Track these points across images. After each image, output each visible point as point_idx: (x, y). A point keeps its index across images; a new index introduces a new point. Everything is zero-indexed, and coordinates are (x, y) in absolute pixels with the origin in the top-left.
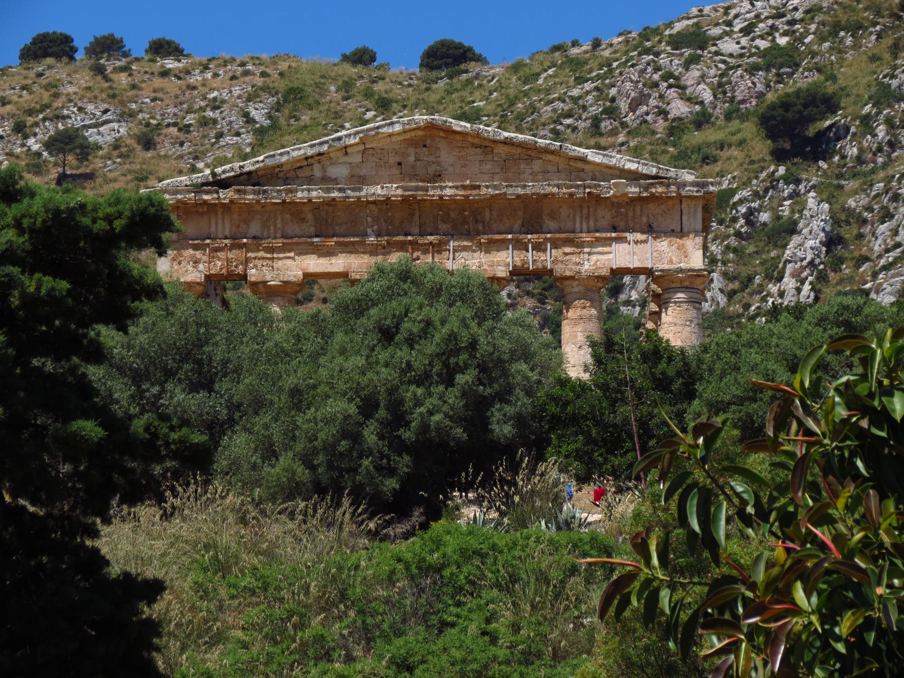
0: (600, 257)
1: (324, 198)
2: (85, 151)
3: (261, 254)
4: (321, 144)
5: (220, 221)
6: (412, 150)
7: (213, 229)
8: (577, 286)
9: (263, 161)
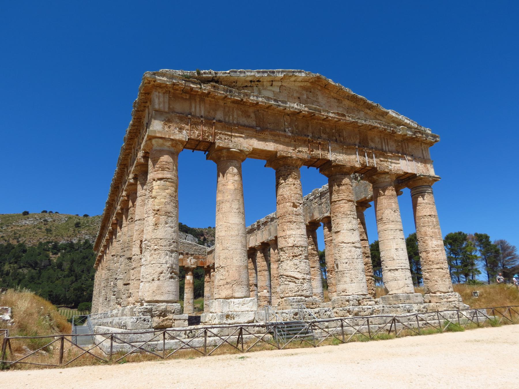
0: (395, 165)
1: (265, 103)
2: (47, 221)
4: (263, 72)
5: (198, 106)
6: (304, 92)
7: (193, 110)
8: (388, 178)
9: (229, 73)
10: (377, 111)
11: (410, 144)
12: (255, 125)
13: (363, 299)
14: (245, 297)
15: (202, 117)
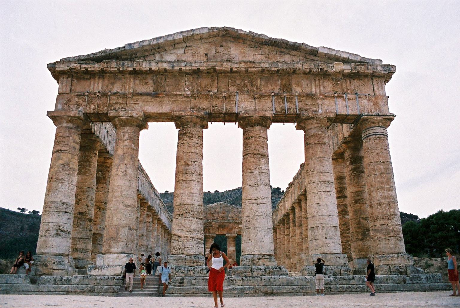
3: (119, 101)
5: (97, 83)
6: (214, 48)
7: (92, 87)
10: (305, 51)
11: (352, 81)
12: (152, 91)
13: (260, 259)
14: (121, 253)
15: (99, 92)
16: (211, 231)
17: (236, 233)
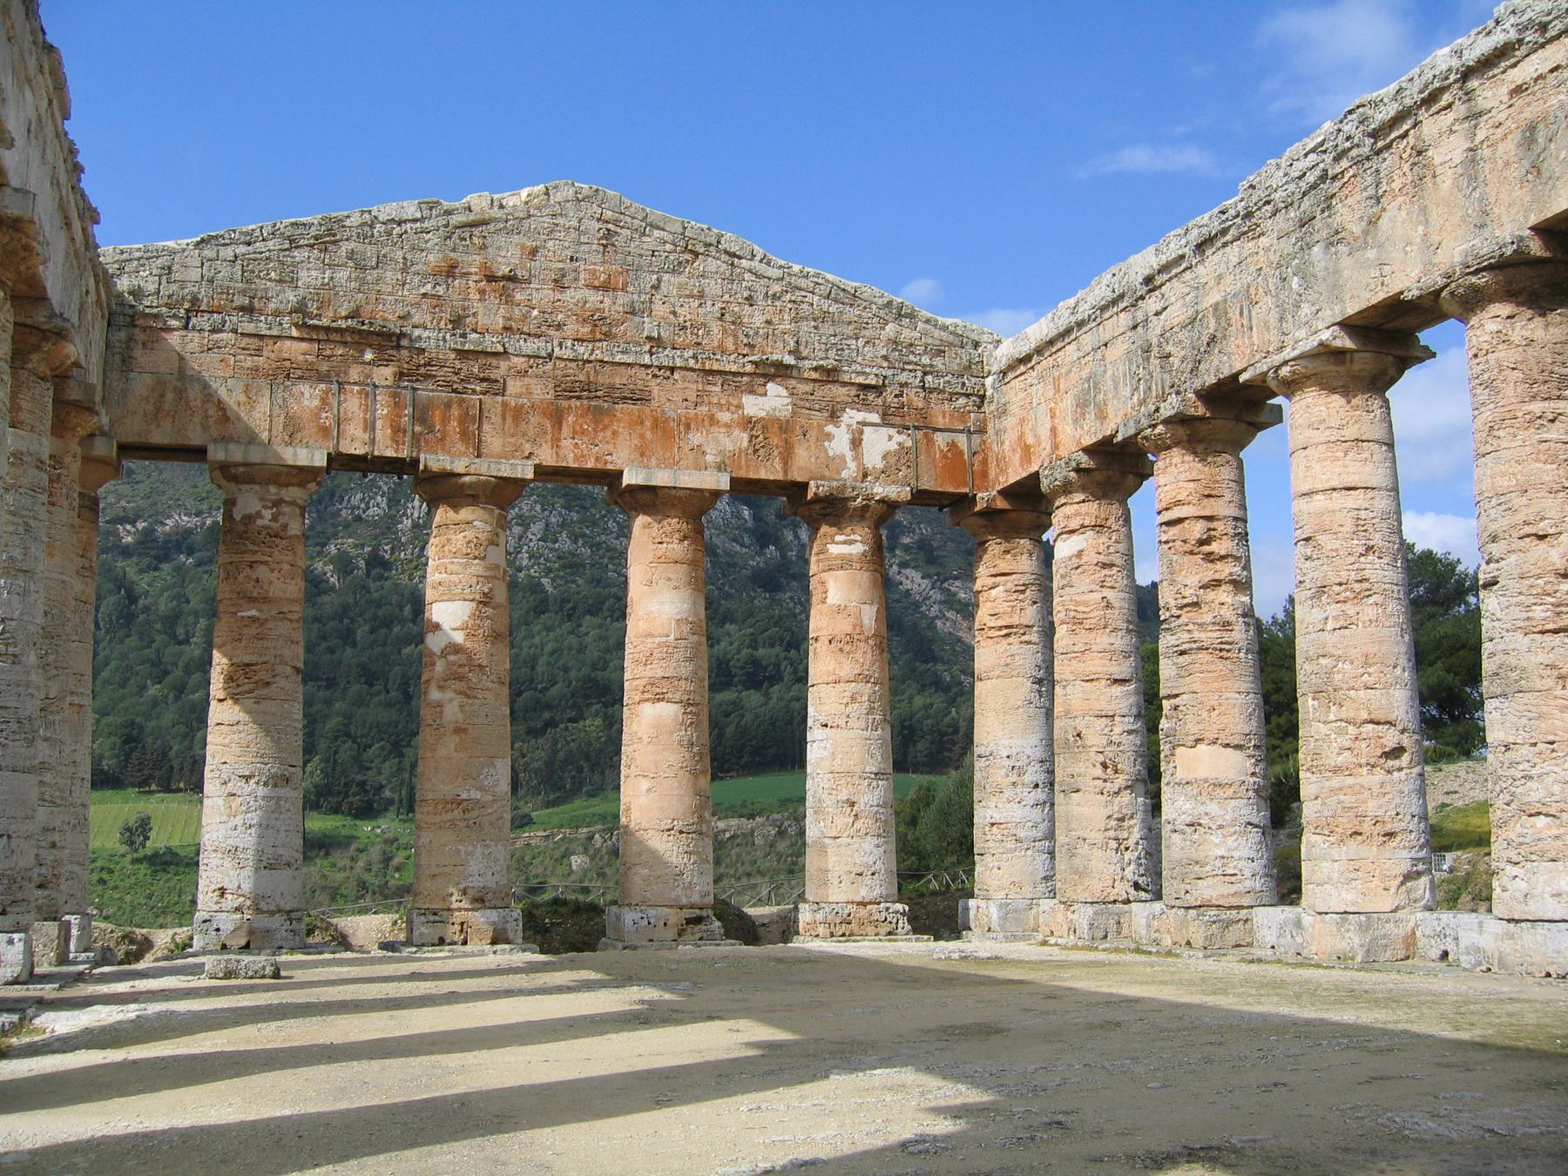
16: (493, 440)
17: (720, 467)
